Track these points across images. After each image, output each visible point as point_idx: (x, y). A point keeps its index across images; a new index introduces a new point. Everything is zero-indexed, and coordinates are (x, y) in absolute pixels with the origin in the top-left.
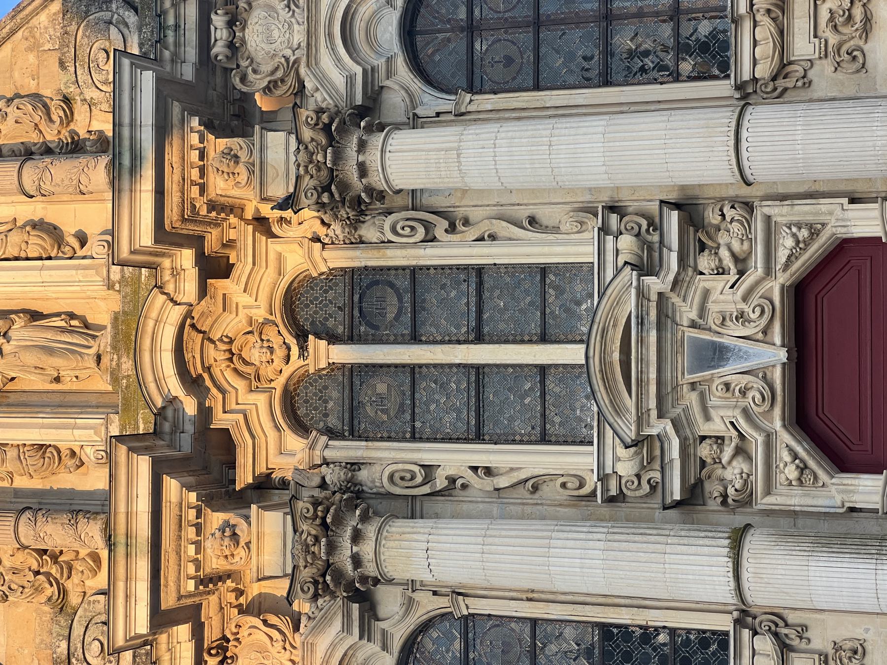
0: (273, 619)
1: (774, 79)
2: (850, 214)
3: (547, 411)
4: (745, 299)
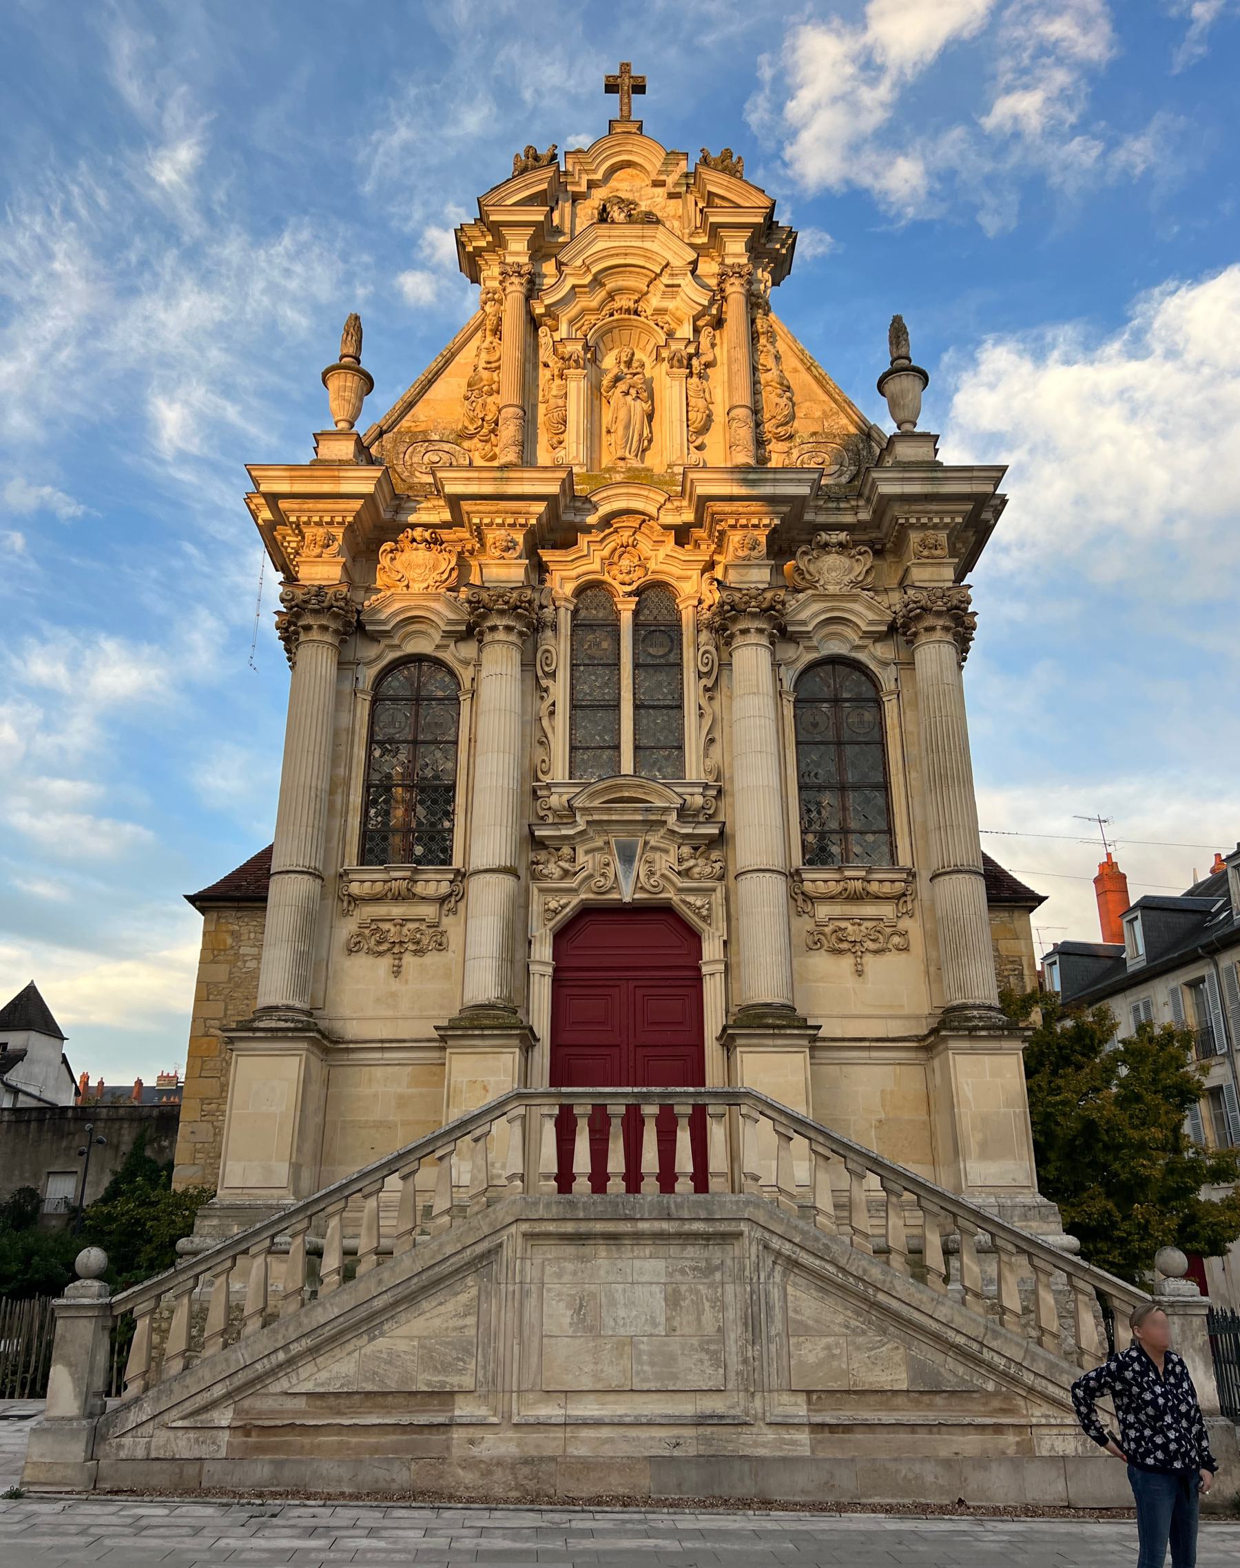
0: (455, 574)
1: (803, 893)
2: (716, 941)
3: (592, 750)
4: (663, 876)
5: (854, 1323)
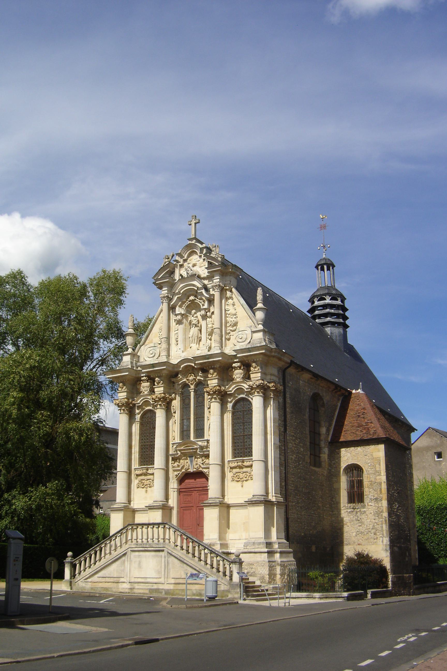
3: (184, 433)
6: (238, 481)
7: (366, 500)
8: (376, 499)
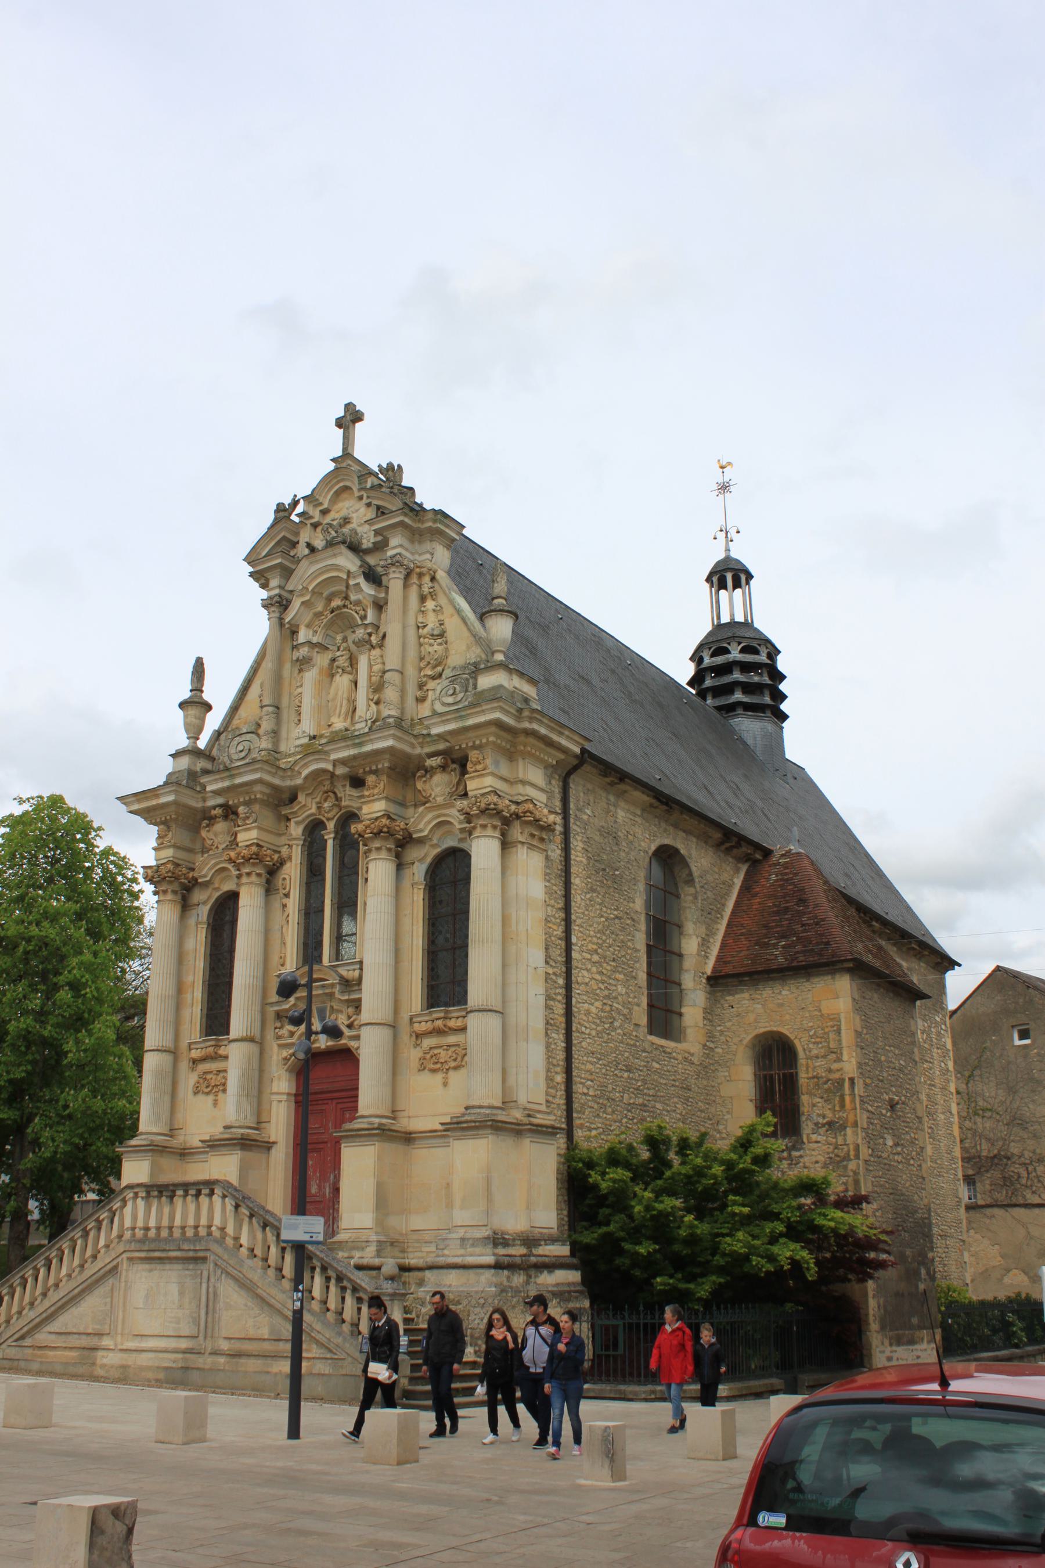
5: (249, 1304)
6: (434, 1071)
7: (807, 1128)
8: (830, 1124)
